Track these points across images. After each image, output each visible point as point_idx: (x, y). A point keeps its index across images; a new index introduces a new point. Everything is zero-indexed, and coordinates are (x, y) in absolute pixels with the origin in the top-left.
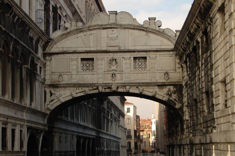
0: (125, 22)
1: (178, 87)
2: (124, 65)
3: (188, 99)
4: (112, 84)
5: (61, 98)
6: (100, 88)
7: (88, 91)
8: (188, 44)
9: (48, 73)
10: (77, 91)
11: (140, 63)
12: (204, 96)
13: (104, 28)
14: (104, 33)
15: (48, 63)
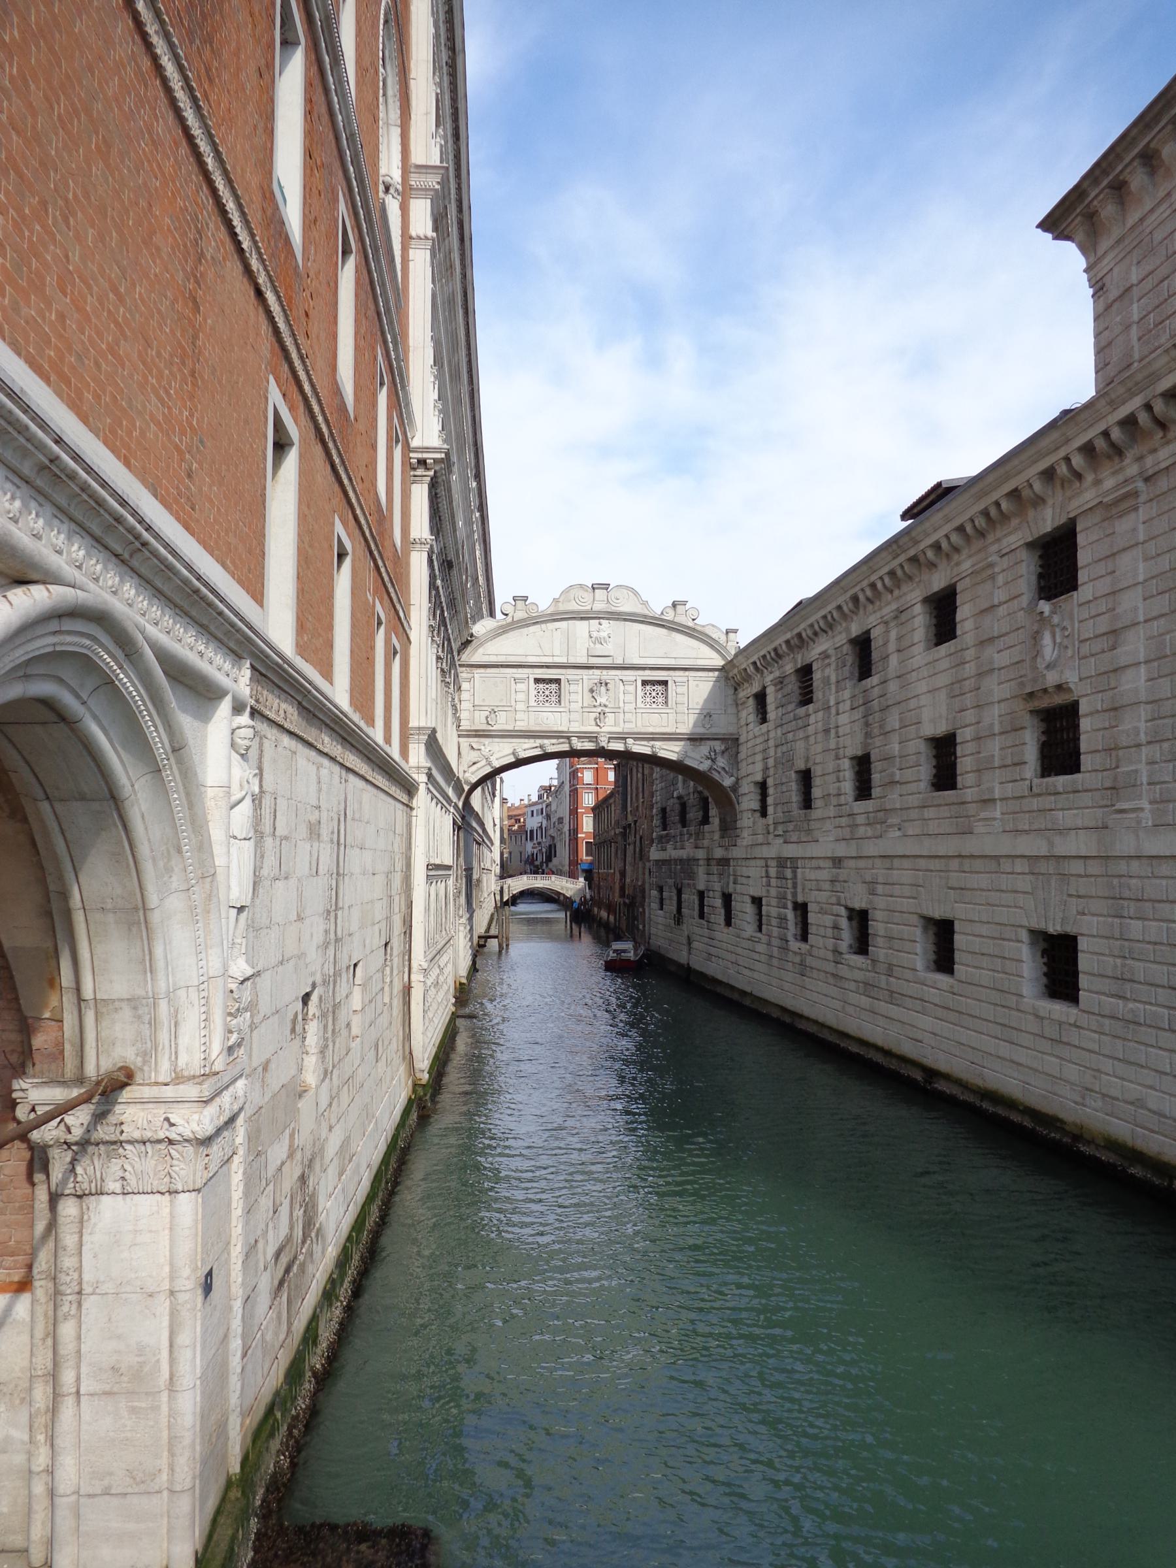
0: (626, 607)
1: (732, 743)
2: (621, 696)
3: (766, 769)
4: (598, 733)
5: (492, 759)
6: (574, 741)
7: (552, 746)
8: (779, 656)
9: (465, 705)
10: (526, 746)
11: (654, 694)
12: (846, 764)
13: (582, 619)
14: (582, 627)
15: (465, 686)
